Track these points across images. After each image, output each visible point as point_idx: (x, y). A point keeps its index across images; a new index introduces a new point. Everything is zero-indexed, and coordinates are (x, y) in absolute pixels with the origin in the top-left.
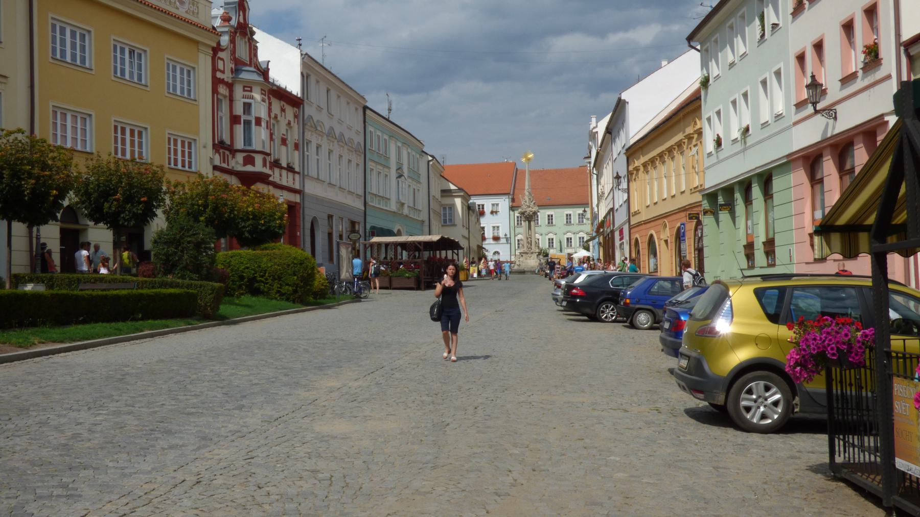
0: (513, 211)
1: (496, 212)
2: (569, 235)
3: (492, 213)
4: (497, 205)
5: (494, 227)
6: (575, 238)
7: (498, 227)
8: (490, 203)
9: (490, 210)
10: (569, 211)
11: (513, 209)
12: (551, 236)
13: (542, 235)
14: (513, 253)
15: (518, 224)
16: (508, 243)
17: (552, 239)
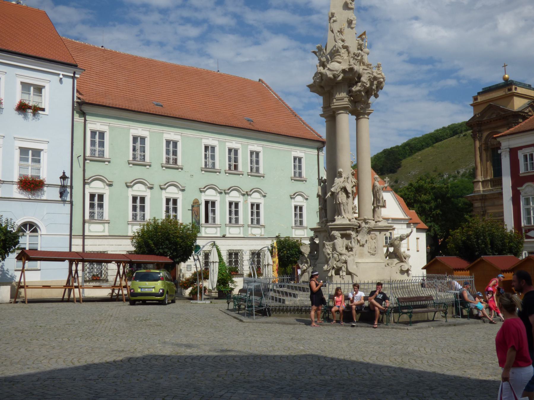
0: (83, 114)
1: (36, 110)
2: (211, 195)
3: (22, 108)
4: (39, 89)
5: (24, 151)
6: (223, 201)
7: (37, 153)
8: (19, 80)
9: (17, 102)
10: (211, 139)
11: (85, 108)
12: (172, 192)
13: (151, 188)
14: (77, 230)
15: (93, 151)
16: (64, 201)
17: (143, 199)
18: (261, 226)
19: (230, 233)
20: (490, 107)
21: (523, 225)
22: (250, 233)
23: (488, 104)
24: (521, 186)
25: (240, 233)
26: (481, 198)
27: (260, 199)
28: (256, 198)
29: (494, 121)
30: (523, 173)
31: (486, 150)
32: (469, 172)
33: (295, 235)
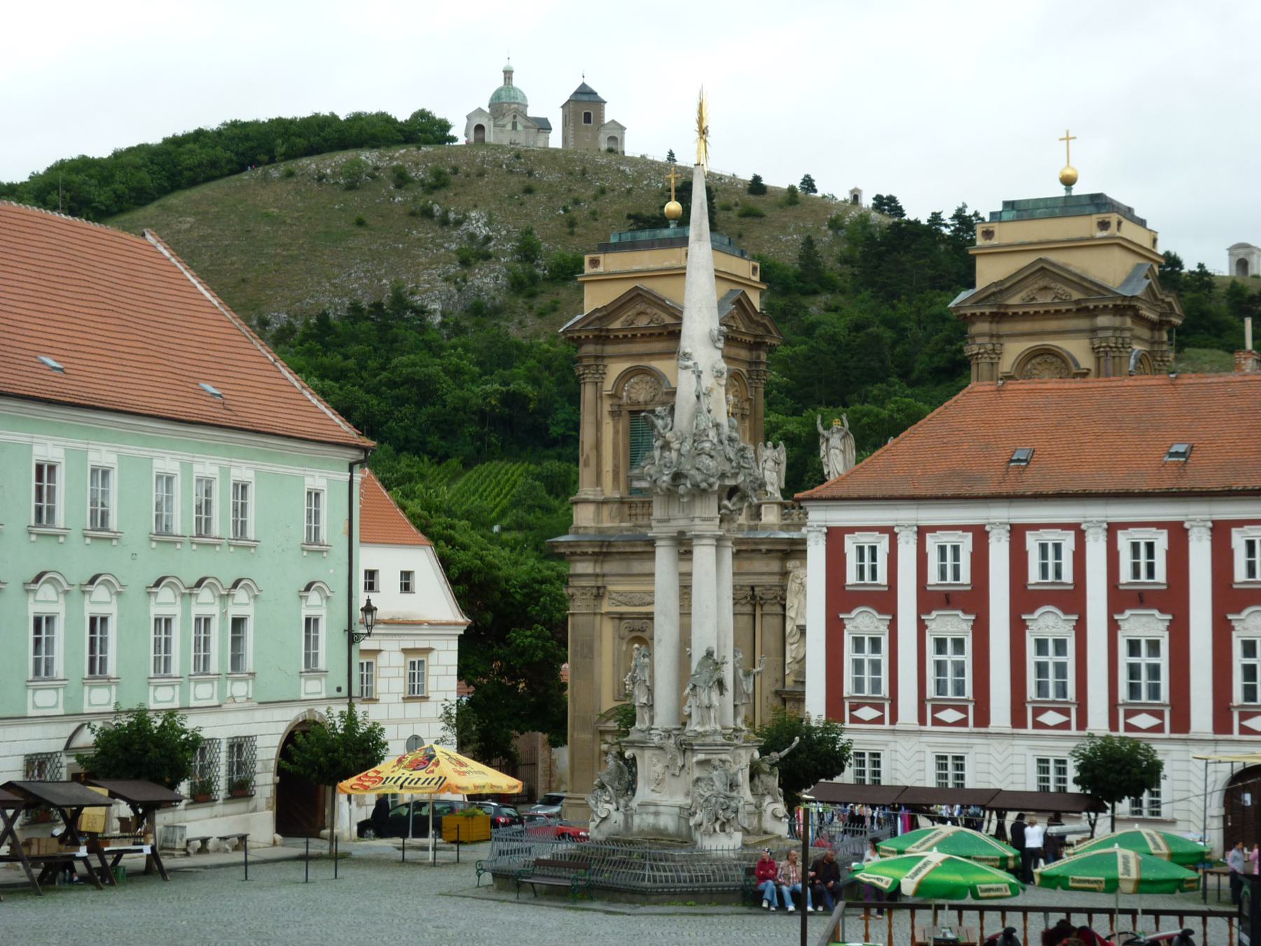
2: (166, 603)
18: (250, 674)
19: (196, 699)
20: (636, 296)
21: (845, 695)
22: (229, 695)
23: (629, 286)
24: (849, 611)
25: (212, 698)
26: (597, 550)
27: (248, 604)
28: (241, 604)
29: (643, 335)
30: (853, 585)
31: (615, 414)
32: (307, 324)
33: (306, 694)
